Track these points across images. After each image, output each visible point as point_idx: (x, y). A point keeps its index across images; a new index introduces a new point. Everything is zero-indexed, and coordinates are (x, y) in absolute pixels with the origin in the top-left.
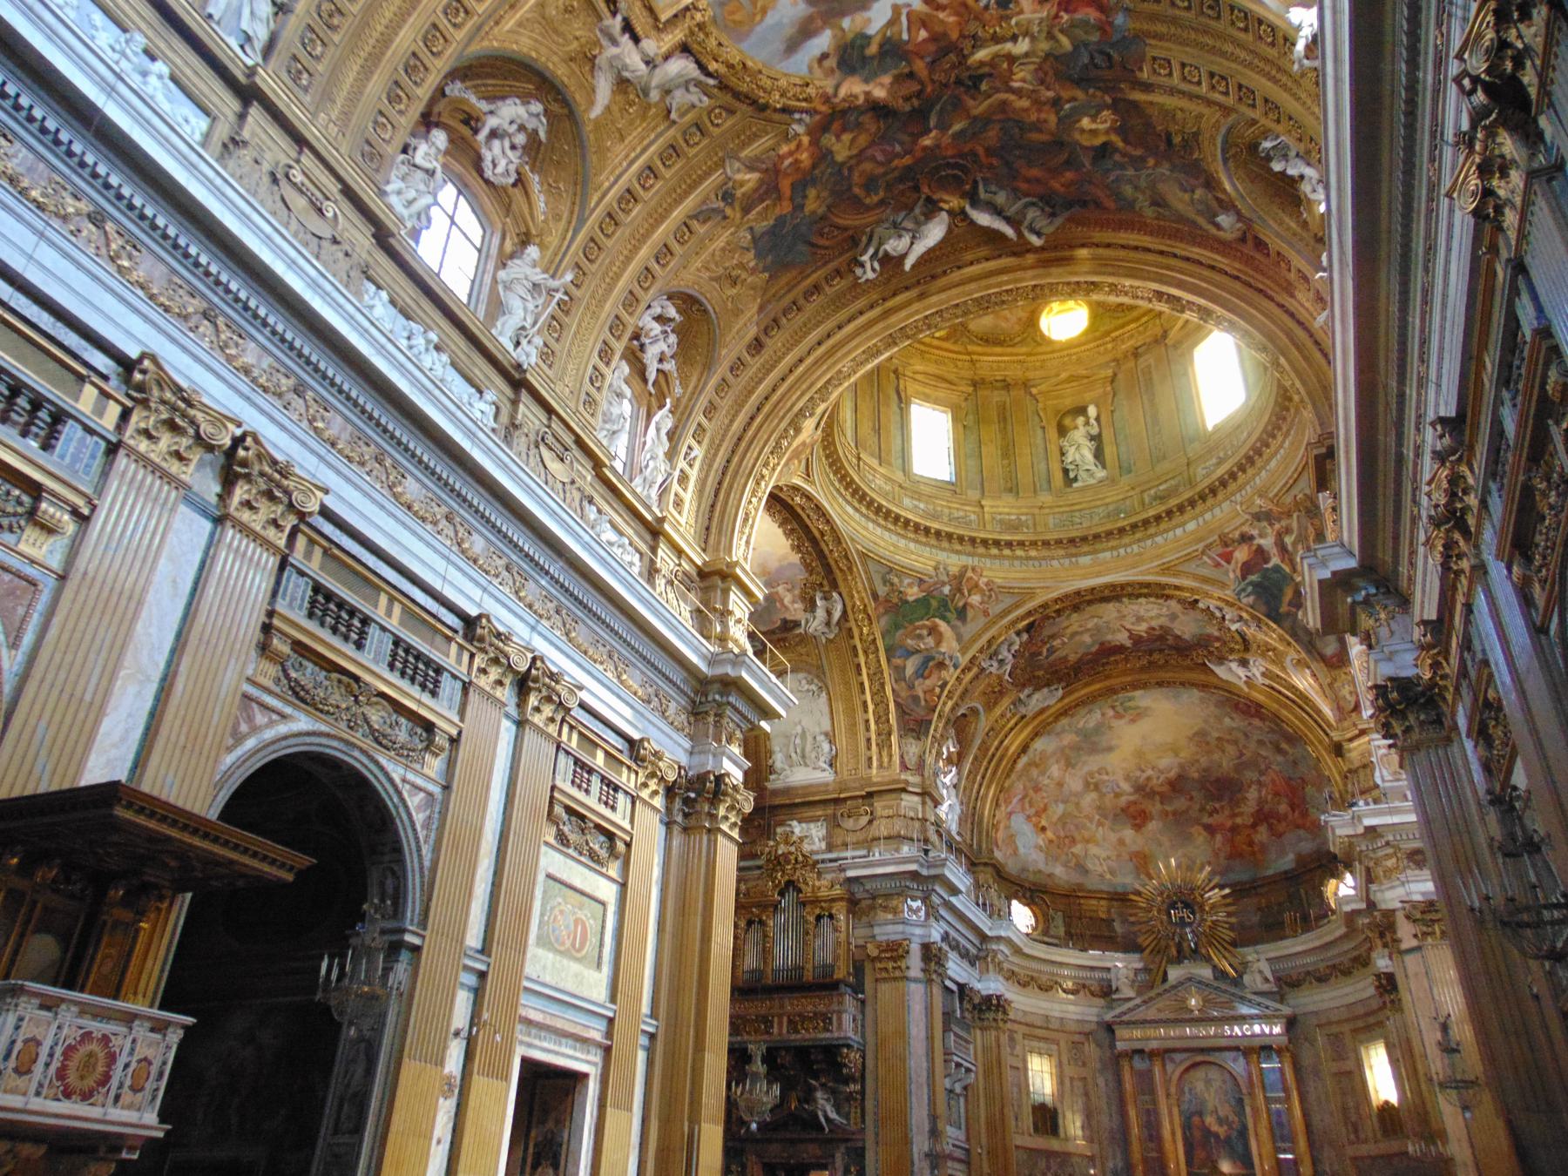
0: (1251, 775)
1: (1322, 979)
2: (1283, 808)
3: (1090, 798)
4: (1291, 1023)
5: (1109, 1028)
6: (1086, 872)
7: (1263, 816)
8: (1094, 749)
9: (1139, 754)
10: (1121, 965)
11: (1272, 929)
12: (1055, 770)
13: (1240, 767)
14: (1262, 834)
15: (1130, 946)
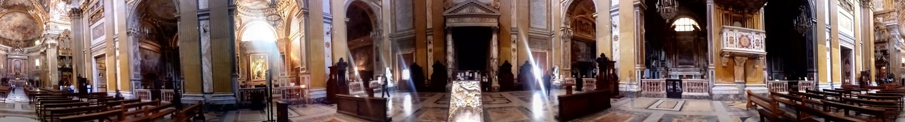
0: (29, 27)
1: (33, 52)
2: (32, 32)
3: (8, 27)
4: (28, 57)
5: (7, 55)
6: (6, 36)
7: (29, 32)
8: (10, 20)
9: (15, 22)
10: (10, 48)
11: (28, 46)
12: (4, 22)
13: (28, 26)
14: (29, 34)
15: (11, 46)
